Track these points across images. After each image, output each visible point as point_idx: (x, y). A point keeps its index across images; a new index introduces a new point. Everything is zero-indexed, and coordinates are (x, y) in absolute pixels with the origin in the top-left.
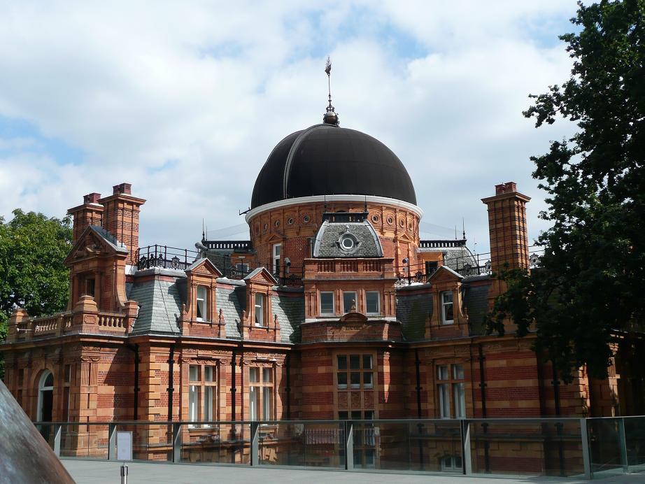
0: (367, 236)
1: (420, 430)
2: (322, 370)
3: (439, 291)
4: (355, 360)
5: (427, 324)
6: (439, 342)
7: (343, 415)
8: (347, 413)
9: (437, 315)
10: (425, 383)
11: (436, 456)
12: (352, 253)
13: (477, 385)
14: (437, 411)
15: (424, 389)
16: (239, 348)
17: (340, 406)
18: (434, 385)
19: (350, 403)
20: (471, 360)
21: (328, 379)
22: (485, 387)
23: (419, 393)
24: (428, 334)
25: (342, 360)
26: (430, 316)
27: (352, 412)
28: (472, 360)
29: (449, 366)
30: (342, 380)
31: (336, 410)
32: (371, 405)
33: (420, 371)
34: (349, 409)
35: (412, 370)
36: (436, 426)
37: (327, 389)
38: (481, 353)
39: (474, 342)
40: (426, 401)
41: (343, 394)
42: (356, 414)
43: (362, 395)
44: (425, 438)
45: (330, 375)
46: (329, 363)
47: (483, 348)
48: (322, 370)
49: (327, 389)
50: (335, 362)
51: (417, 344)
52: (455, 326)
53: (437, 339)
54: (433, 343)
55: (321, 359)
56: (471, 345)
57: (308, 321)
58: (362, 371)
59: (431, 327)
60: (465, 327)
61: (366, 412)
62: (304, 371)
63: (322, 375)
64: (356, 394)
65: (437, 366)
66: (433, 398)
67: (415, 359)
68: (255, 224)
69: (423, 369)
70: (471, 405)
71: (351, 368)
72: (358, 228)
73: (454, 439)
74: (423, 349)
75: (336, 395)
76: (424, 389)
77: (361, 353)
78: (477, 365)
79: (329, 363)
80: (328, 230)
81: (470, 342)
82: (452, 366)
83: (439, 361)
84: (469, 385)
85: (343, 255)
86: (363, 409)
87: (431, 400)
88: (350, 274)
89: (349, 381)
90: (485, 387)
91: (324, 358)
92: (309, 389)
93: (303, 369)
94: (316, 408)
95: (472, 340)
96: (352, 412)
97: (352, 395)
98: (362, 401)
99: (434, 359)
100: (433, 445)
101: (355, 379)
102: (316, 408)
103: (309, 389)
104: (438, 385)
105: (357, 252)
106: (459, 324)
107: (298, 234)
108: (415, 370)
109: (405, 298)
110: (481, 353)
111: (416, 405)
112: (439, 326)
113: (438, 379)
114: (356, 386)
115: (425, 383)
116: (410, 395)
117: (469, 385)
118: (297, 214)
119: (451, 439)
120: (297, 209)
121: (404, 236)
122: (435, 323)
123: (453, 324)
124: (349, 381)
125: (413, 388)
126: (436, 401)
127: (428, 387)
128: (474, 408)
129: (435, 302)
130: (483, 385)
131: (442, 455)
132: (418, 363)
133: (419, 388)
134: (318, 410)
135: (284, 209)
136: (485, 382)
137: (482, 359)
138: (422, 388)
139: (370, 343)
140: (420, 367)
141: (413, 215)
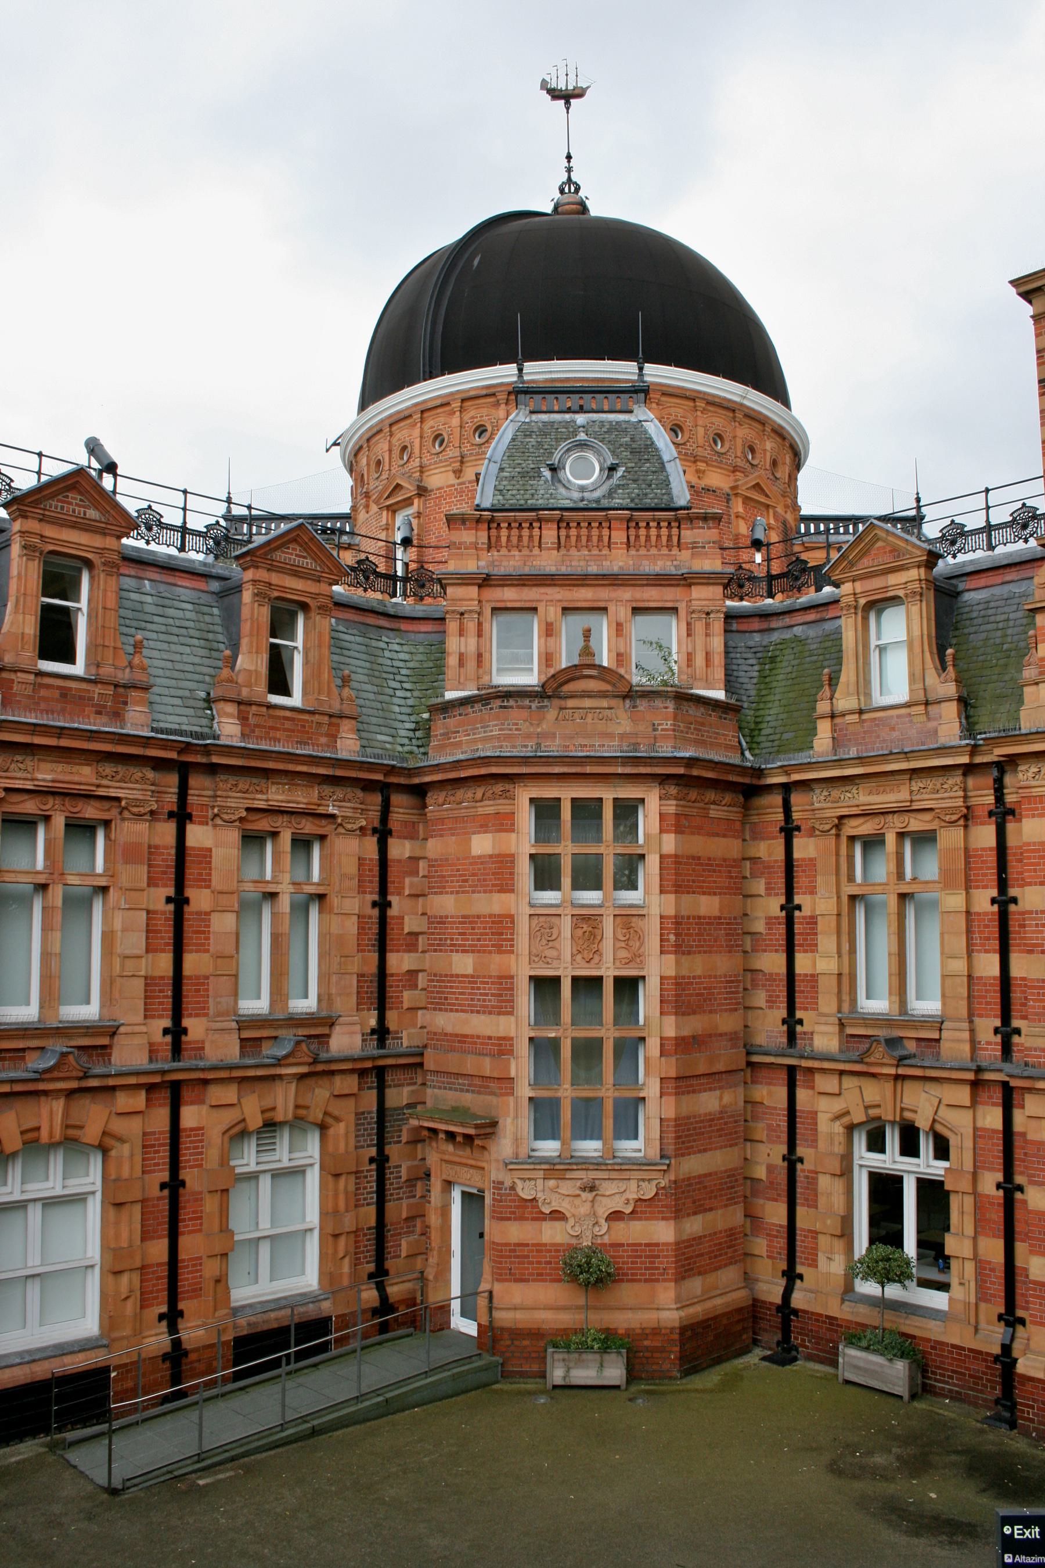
0: (645, 450)
1: (792, 1037)
2: (482, 844)
3: (862, 601)
4: (587, 812)
5: (823, 707)
6: (861, 760)
7: (545, 987)
8: (556, 981)
9: (853, 679)
10: (812, 891)
11: (837, 1117)
12: (597, 494)
13: (984, 900)
14: (845, 981)
15: (806, 911)
16: (186, 763)
17: (534, 957)
18: (839, 897)
19: (566, 947)
20: (965, 817)
21: (498, 873)
22: (1012, 907)
23: (790, 922)
24: (824, 728)
25: (546, 812)
26: (833, 681)
27: (575, 980)
28: (967, 818)
29: (891, 839)
30: (546, 874)
31: (523, 969)
32: (636, 958)
33: (796, 855)
34: (566, 967)
35: (771, 850)
36: (842, 1025)
37: (494, 904)
38: (999, 798)
39: (978, 760)
40: (813, 948)
41: (544, 921)
42: (587, 986)
43: (608, 925)
44: (804, 1063)
45: (504, 862)
46: (505, 823)
47: (1008, 780)
48: (482, 844)
49: (494, 904)
50: (526, 819)
51: (786, 770)
52: (915, 710)
53: (853, 753)
54: (839, 762)
55: (481, 811)
56: (968, 769)
57: (450, 695)
58: (608, 849)
59: (833, 716)
60: (950, 711)
61: (619, 981)
62: (434, 847)
63: (481, 859)
64: (588, 922)
65: (852, 839)
66: (834, 938)
67: (781, 817)
68: (359, 455)
69: (804, 848)
70: (959, 966)
71: (574, 840)
72: (616, 428)
73: (901, 1071)
74: (805, 785)
75: (523, 927)
76: (806, 911)
77: (608, 794)
78: (985, 836)
79: (505, 823)
80: (525, 431)
81: (965, 760)
82: (901, 835)
83: (854, 822)
84: (956, 901)
85: (567, 504)
86: (608, 970)
87: (827, 942)
88: (579, 561)
89: (566, 881)
90: (1012, 907)
91: (488, 808)
92: (446, 904)
93: (431, 843)
94: (463, 964)
95: (974, 750)
96: (575, 980)
97: (575, 927)
98: (608, 945)
99: (841, 818)
100: (827, 1083)
101: (588, 876)
102: (463, 964)
103: (446, 904)
104: (853, 898)
105: (610, 494)
106: (927, 703)
107: (458, 473)
108: (780, 854)
109: (757, 637)
110: (999, 798)
111: (781, 958)
112: (861, 712)
113: (851, 878)
114: (591, 897)
115: (812, 891)
116: (760, 927)
117: (956, 901)
118: (455, 421)
119: (892, 1071)
120: (456, 405)
121: (757, 487)
122: (844, 702)
123: (907, 705)
124: (566, 881)
125: (774, 905)
126: (846, 947)
127: (818, 902)
128: (970, 977)
129: (849, 638)
130: (1004, 902)
131: (858, 1117)
132: (789, 831)
133: (790, 908)
134: (470, 971)
135: (425, 411)
136: (1013, 892)
137: (1003, 814)
138: (799, 908)
139: (636, 761)
140: (796, 841)
141: (784, 439)
